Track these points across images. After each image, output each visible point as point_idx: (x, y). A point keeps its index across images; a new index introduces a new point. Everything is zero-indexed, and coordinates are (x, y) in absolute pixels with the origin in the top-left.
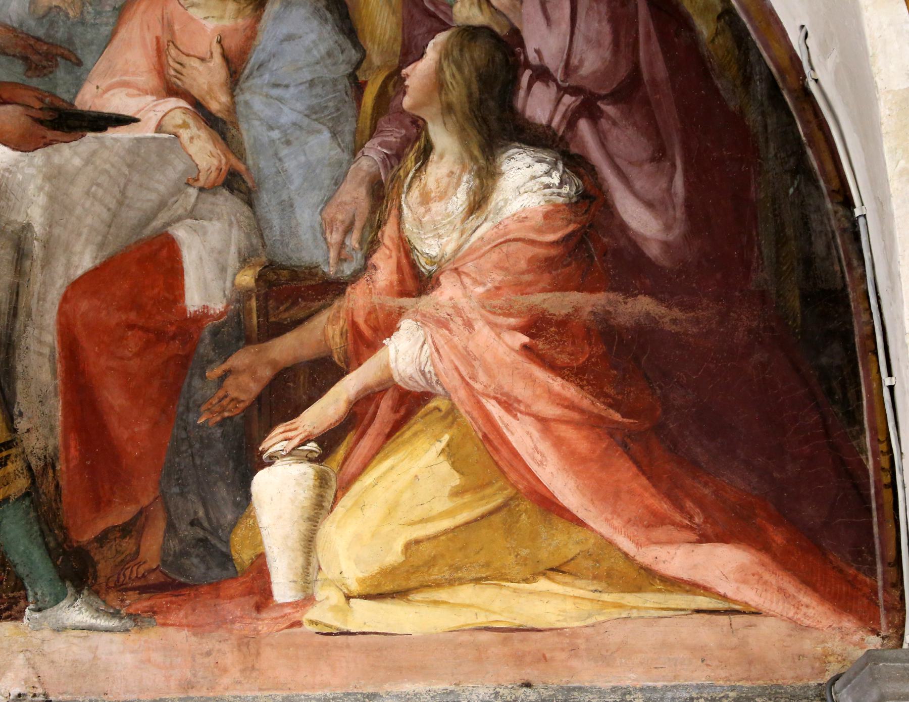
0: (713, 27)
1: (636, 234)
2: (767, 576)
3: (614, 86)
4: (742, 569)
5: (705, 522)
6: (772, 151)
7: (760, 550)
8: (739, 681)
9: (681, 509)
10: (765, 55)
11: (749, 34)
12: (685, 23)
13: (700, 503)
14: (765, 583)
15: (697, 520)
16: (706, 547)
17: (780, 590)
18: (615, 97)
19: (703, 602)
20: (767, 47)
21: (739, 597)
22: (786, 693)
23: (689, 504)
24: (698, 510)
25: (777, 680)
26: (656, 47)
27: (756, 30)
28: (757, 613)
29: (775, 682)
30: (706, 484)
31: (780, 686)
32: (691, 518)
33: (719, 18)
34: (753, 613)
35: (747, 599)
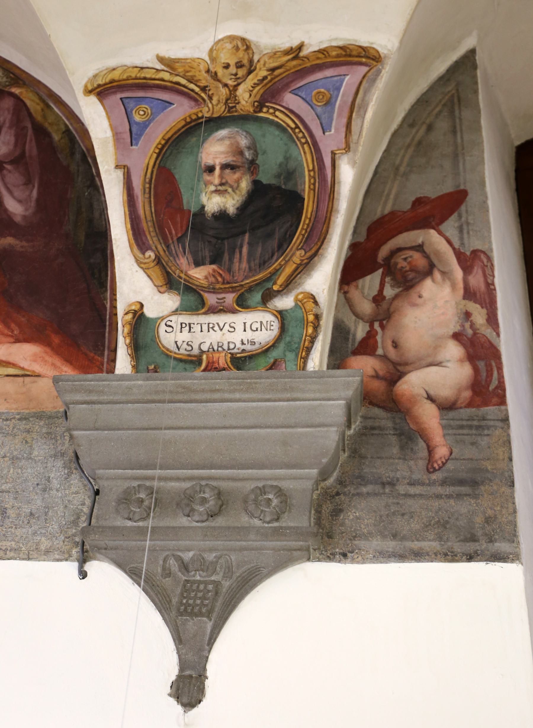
0: (60, 136)
1: (11, 213)
2: (47, 358)
3: (12, 158)
4: (35, 355)
5: (20, 333)
6: (80, 179)
7: (46, 346)
8: (23, 409)
9: (8, 327)
10: (82, 145)
11: (75, 138)
12: (48, 135)
13: (19, 325)
14: (46, 361)
15: (15, 332)
16: (18, 345)
17: (53, 365)
18: (11, 162)
19: (11, 371)
20: (83, 142)
21: (30, 369)
22: (46, 415)
23: (13, 325)
24: (17, 328)
25: (43, 409)
26: (34, 143)
27: (79, 136)
28: (39, 376)
29: (42, 410)
30: (24, 316)
31: (44, 412)
32: (13, 331)
33: (64, 133)
34: (37, 376)
35: (34, 369)
